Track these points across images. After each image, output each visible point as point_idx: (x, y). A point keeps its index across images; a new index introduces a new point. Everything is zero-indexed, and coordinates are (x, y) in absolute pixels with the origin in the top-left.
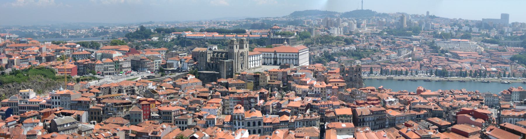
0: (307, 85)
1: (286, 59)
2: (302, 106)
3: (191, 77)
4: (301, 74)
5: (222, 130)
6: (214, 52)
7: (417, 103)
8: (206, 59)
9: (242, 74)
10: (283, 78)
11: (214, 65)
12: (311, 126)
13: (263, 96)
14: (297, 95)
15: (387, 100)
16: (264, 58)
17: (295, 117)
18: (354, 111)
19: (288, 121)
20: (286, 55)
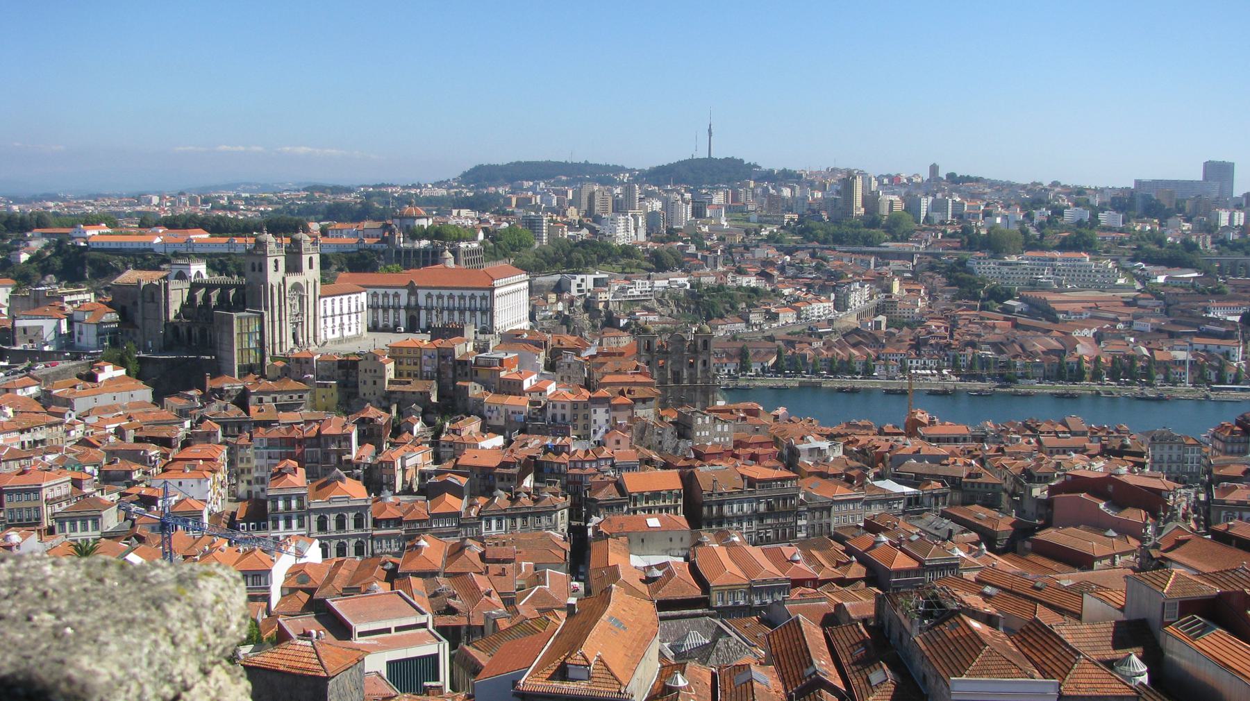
0: (521, 393)
1: (451, 310)
2: (504, 465)
3: (109, 372)
4: (502, 355)
5: (230, 544)
6: (195, 287)
7: (908, 457)
8: (167, 311)
9: (298, 360)
10: (439, 371)
11: (196, 331)
12: (539, 529)
13: (369, 434)
14: (487, 429)
15: (803, 447)
16: (373, 307)
17: (481, 501)
18: (689, 480)
19: (458, 514)
20: (451, 297)
